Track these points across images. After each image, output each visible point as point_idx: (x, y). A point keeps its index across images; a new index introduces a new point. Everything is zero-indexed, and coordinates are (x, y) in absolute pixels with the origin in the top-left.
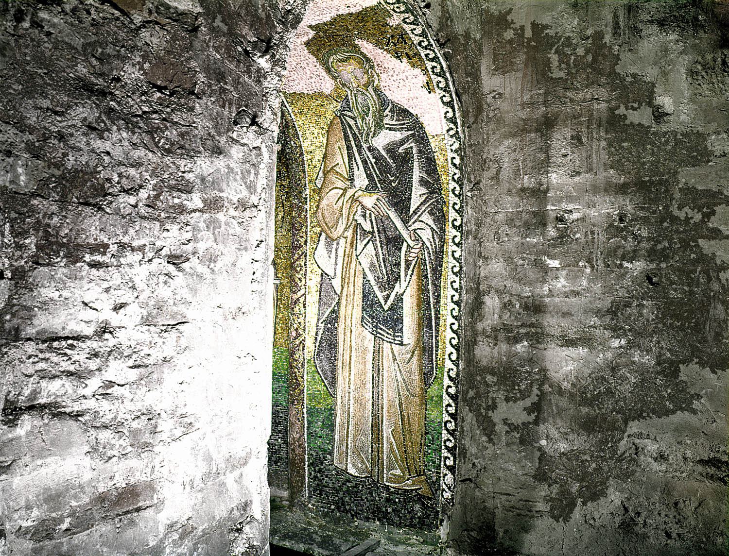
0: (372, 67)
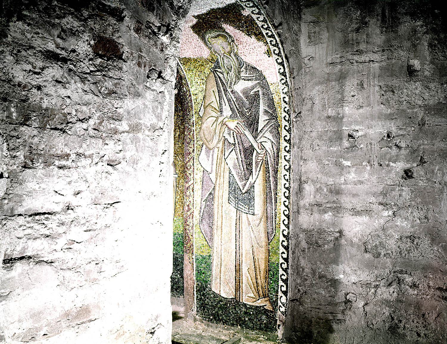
0: (233, 41)
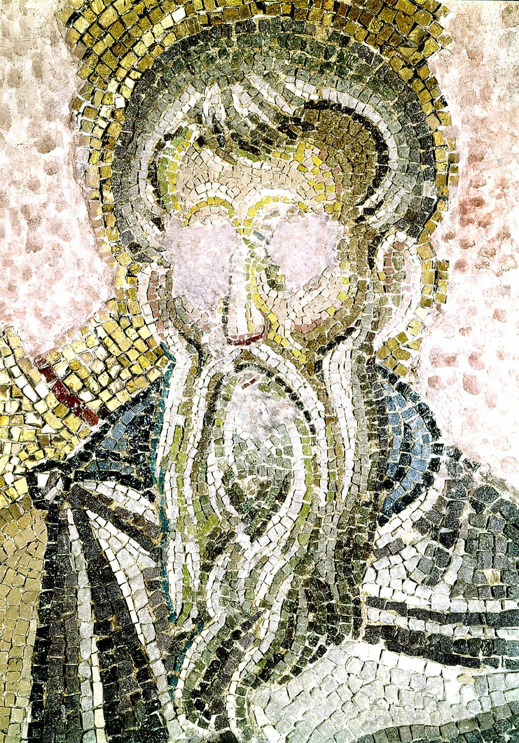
0: (417, 220)
